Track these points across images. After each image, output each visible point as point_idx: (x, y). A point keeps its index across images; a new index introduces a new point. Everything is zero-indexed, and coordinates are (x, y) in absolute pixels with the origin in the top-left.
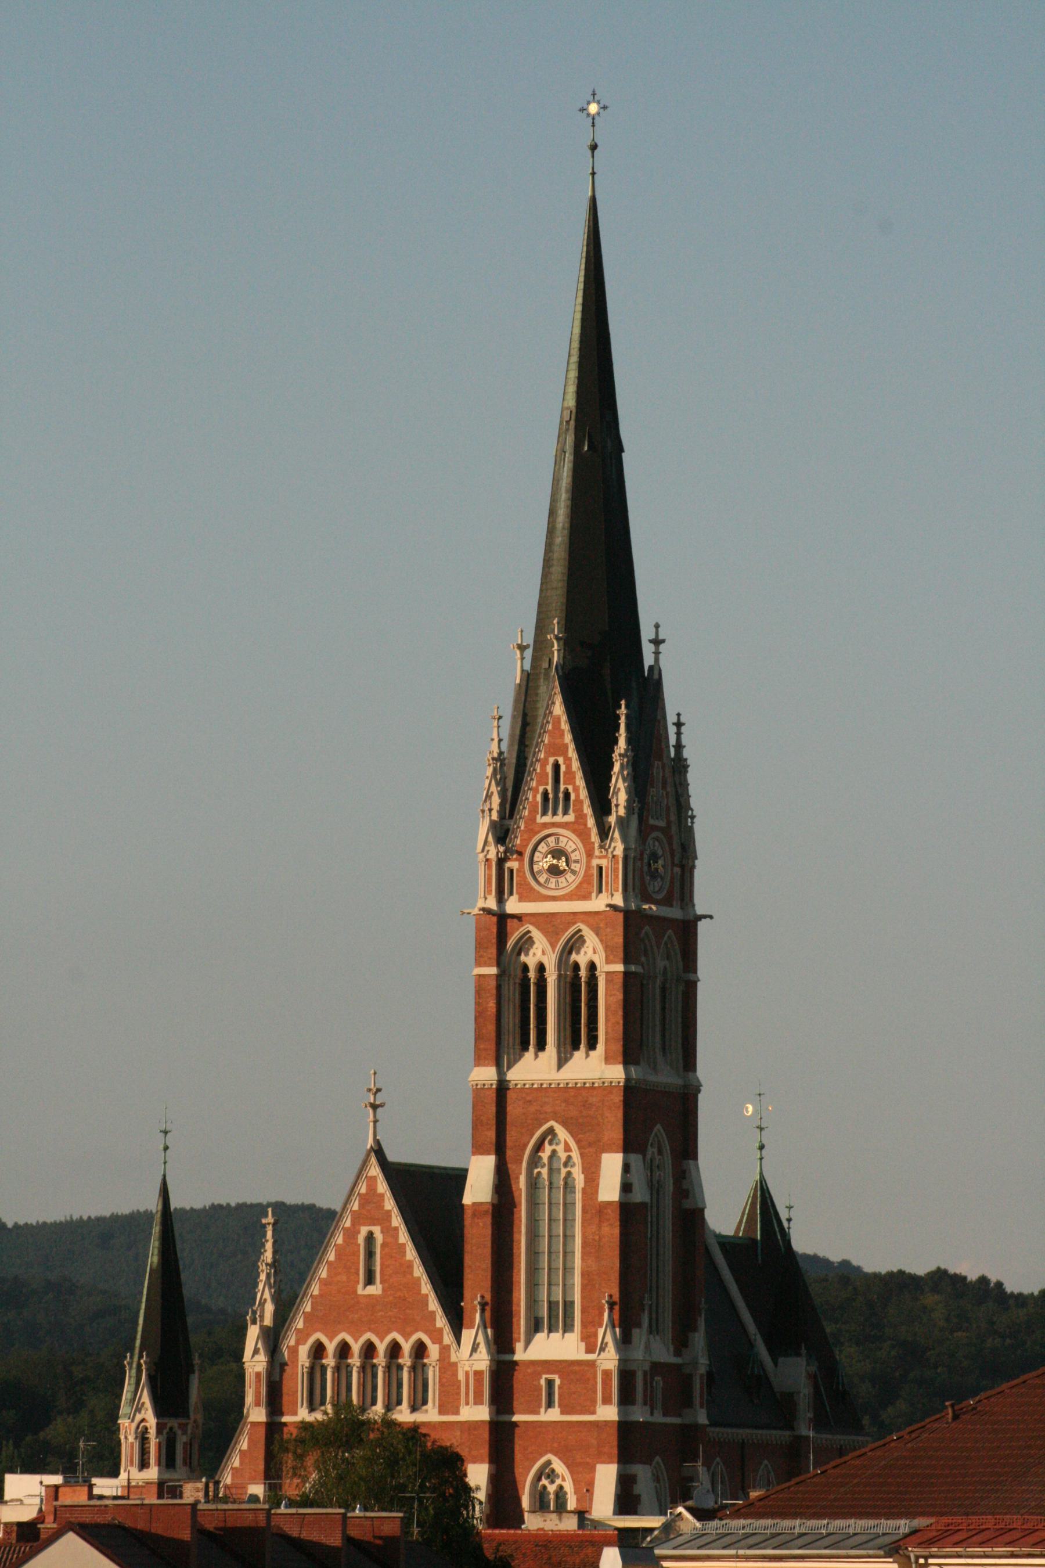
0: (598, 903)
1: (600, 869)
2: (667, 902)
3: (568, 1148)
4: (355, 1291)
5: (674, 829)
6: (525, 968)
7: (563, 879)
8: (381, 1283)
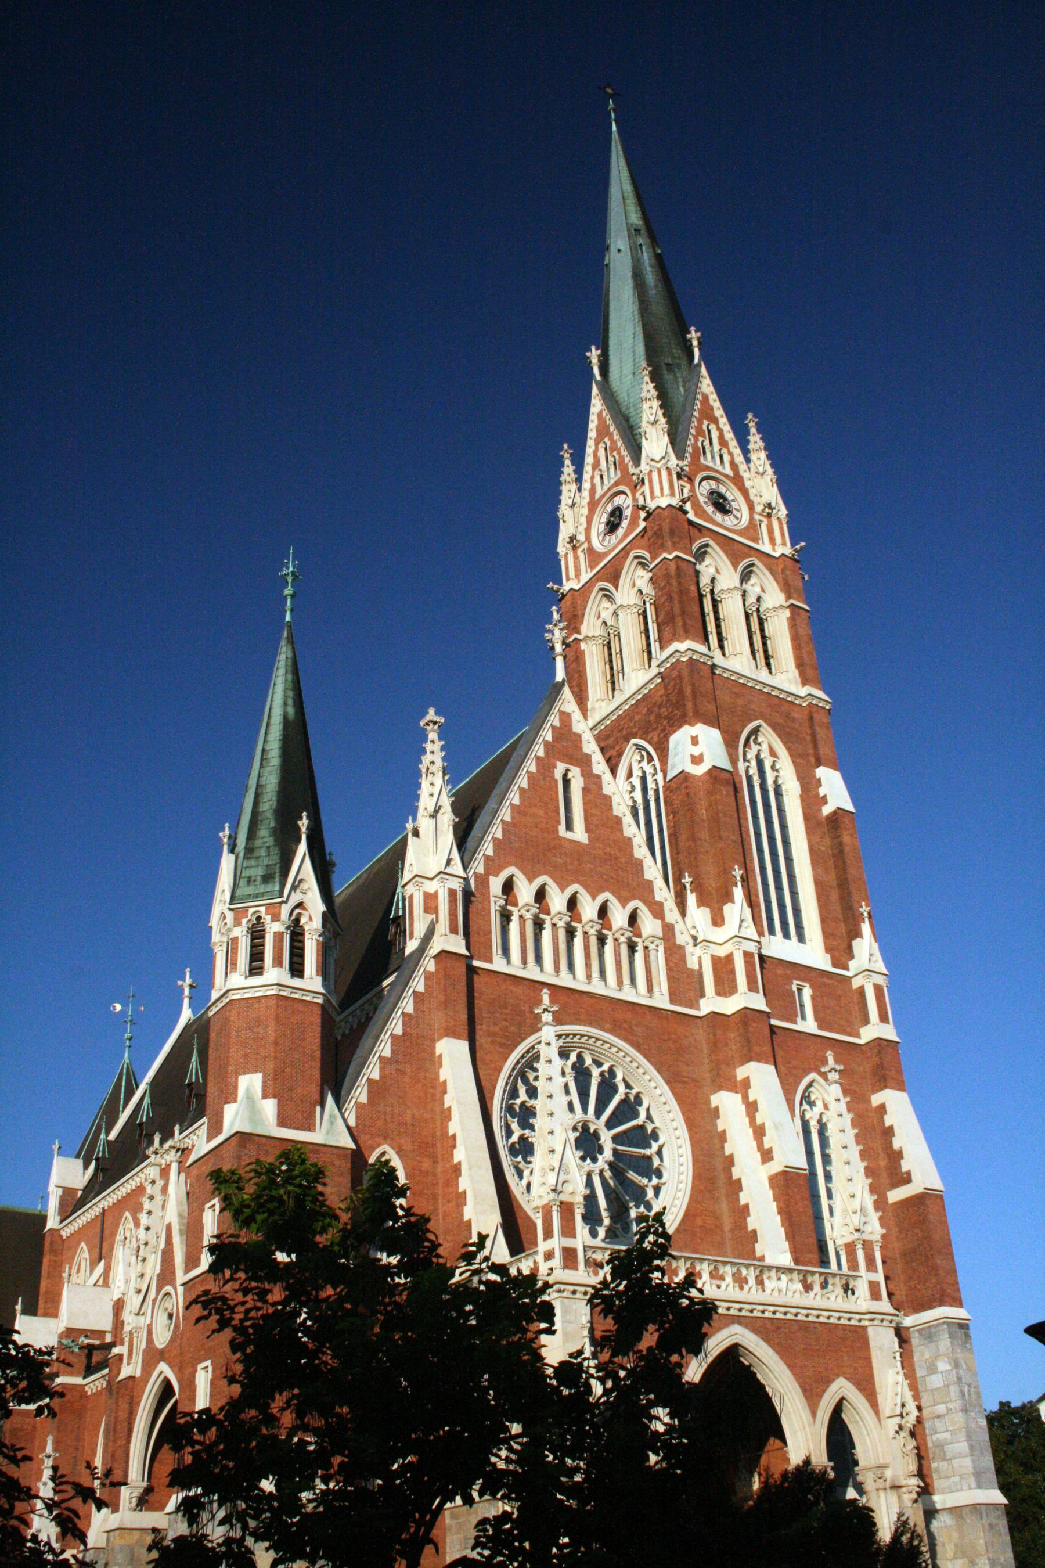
3: (773, 753)
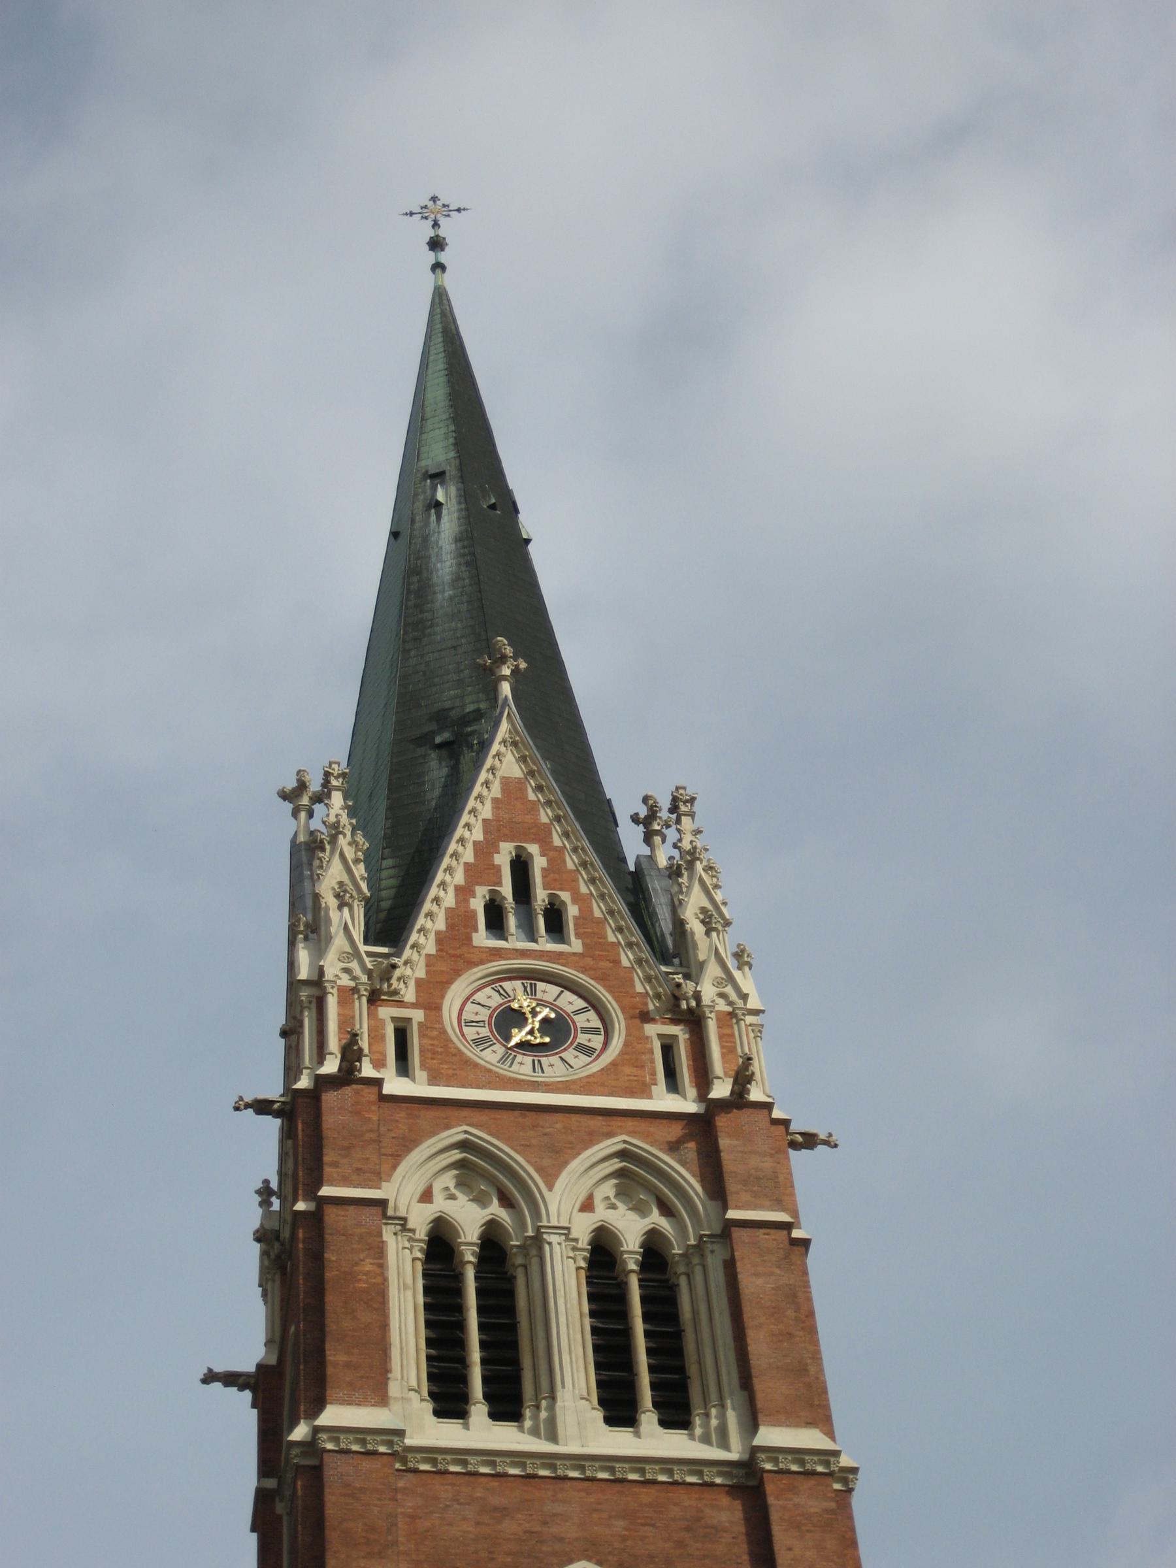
7: (555, 1060)
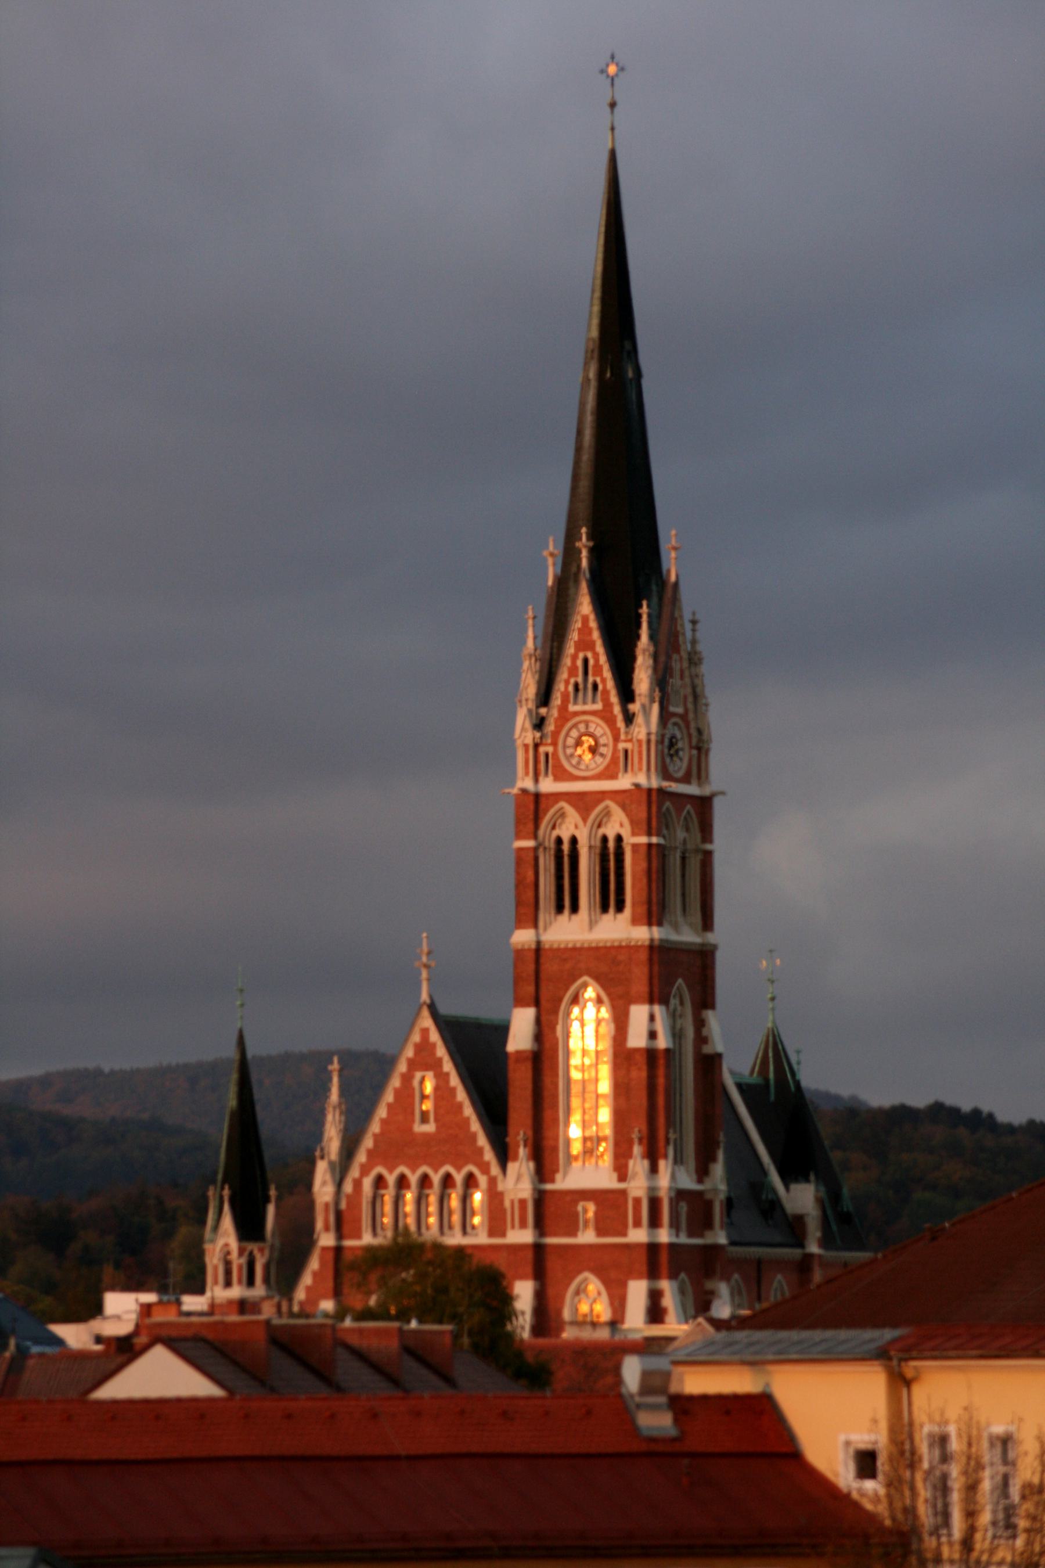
0: (624, 782)
1: (626, 751)
2: (686, 779)
4: (410, 1129)
5: (691, 716)
6: (559, 841)
8: (436, 1120)
